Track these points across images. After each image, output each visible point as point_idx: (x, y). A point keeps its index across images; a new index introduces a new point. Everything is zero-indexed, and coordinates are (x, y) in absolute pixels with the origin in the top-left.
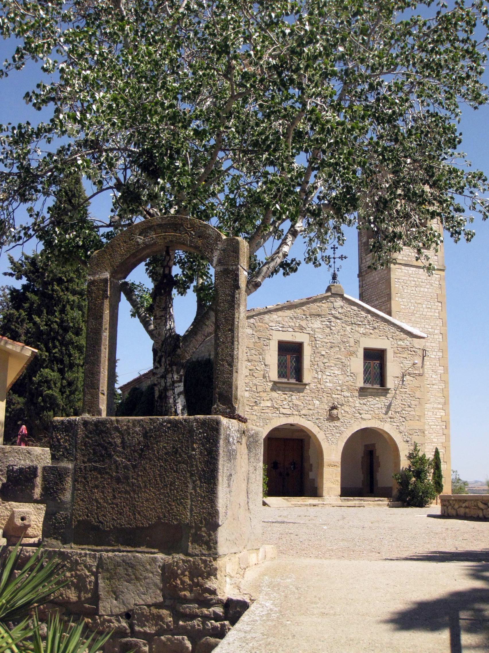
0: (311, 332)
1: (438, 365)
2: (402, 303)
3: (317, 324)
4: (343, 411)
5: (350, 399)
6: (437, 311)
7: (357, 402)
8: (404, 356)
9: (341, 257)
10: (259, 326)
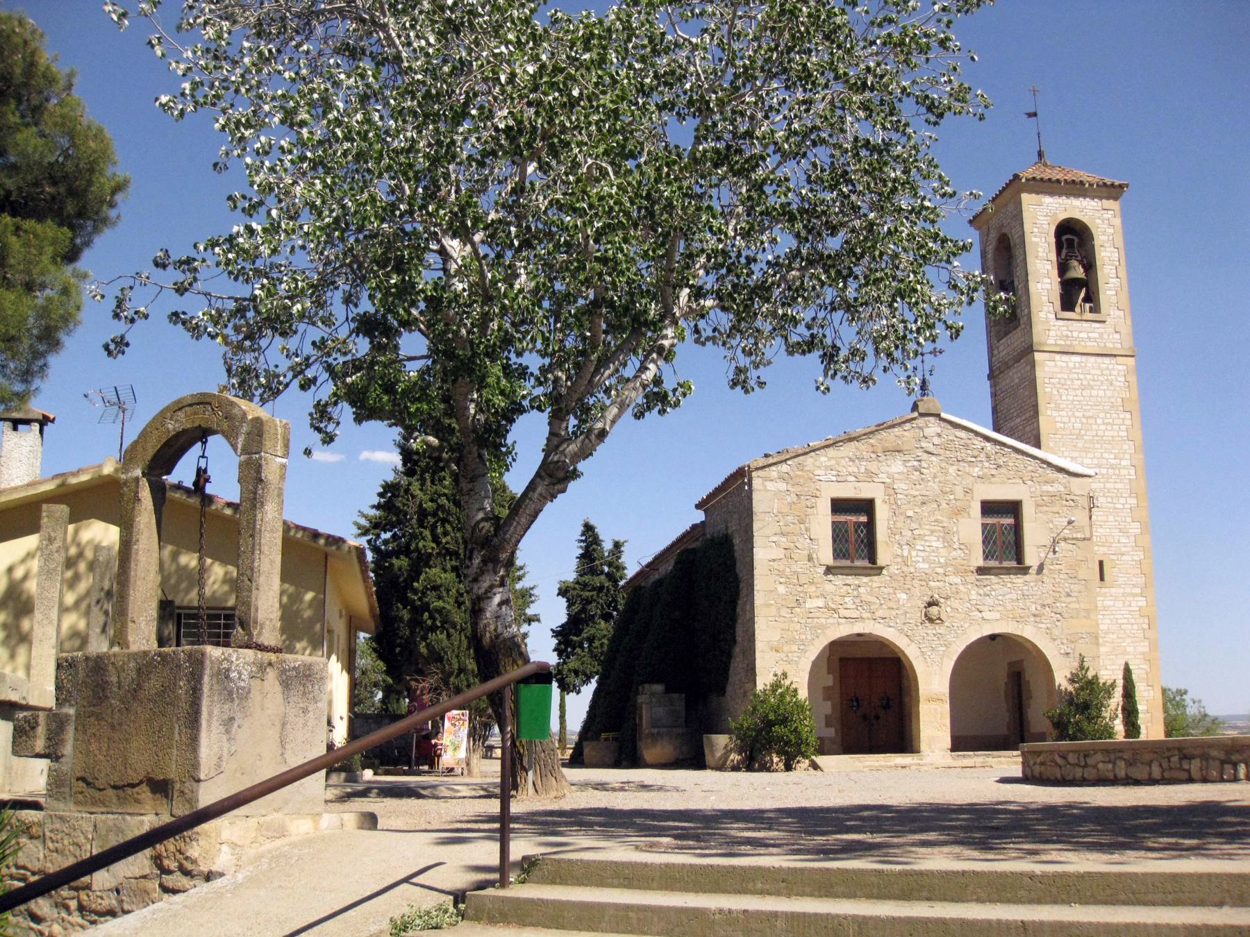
0: (888, 481)
1: (1129, 520)
2: (1058, 419)
3: (897, 466)
4: (949, 609)
5: (961, 587)
6: (1123, 428)
7: (973, 592)
8: (1055, 509)
10: (797, 476)
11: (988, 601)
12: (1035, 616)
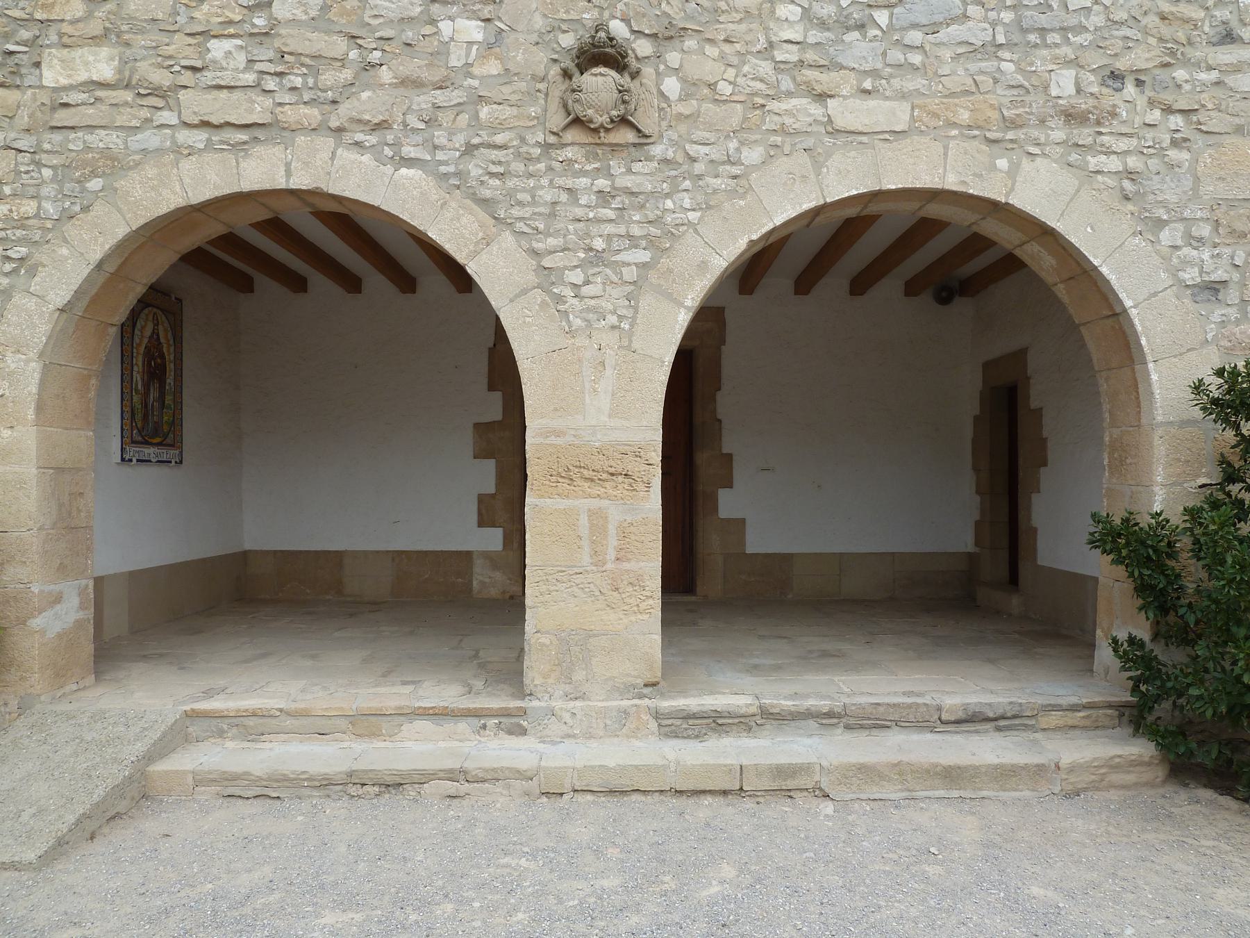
11: (859, 50)
12: (1072, 117)
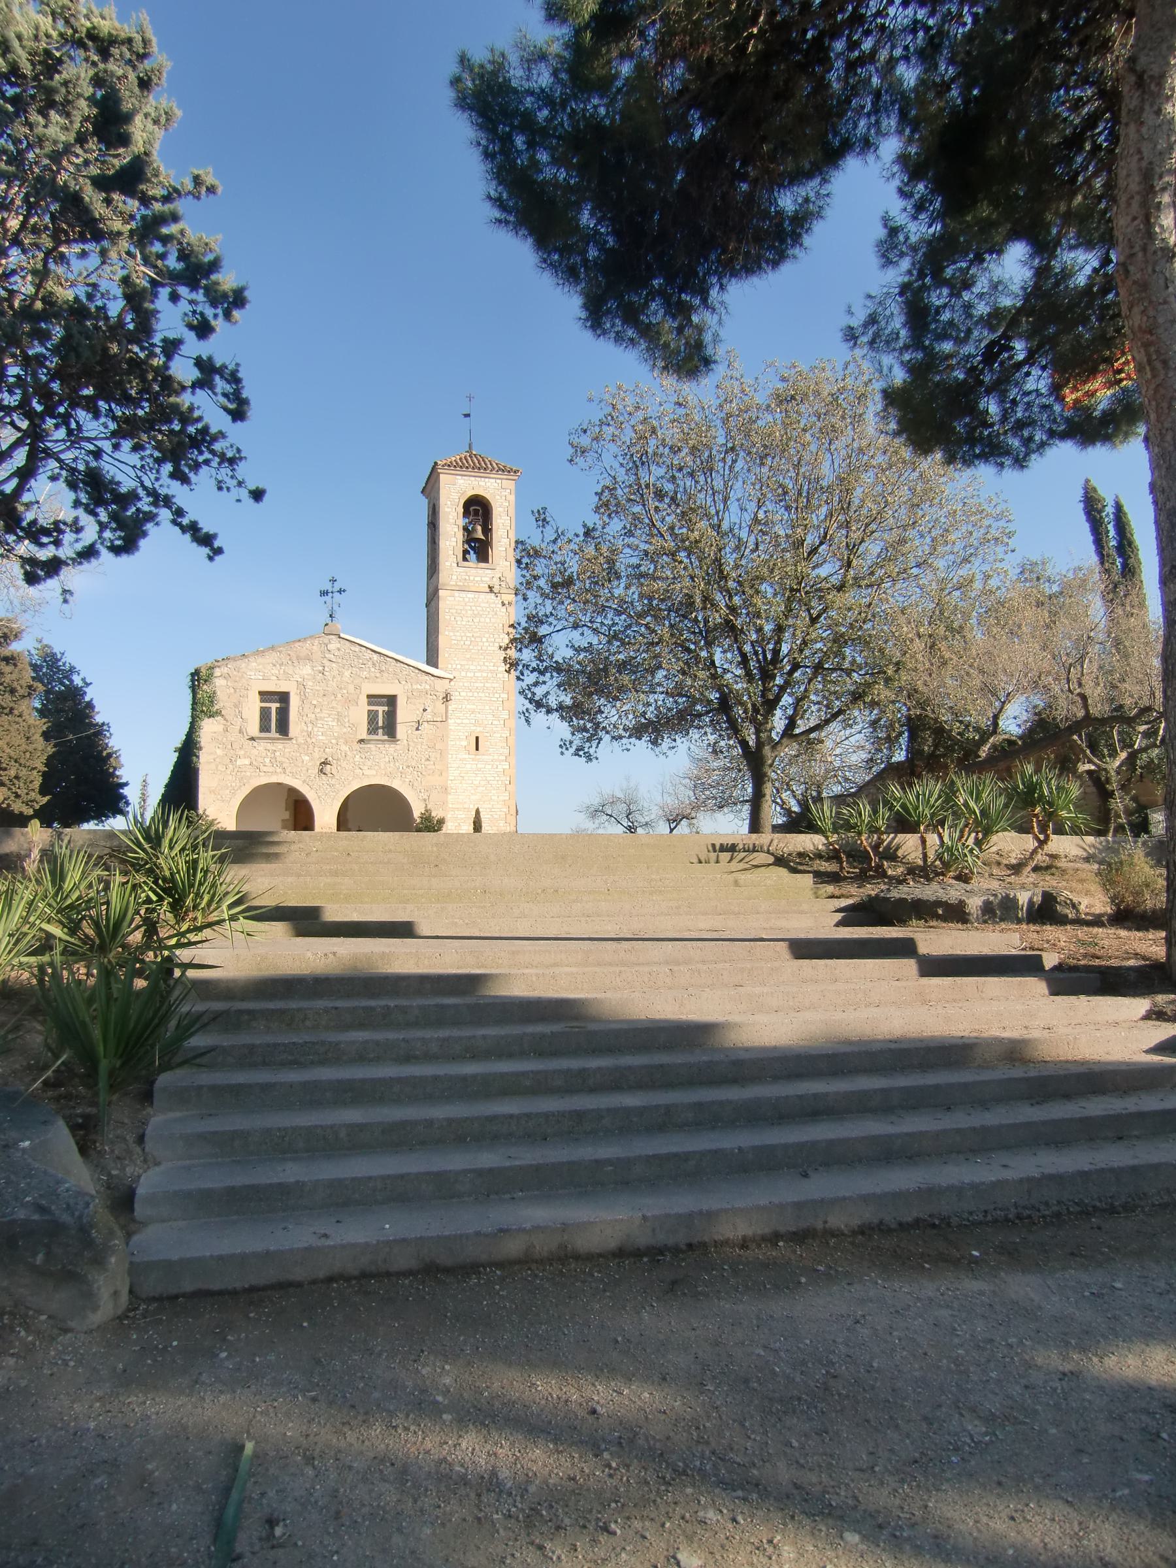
3: (307, 670)
9: (340, 591)
